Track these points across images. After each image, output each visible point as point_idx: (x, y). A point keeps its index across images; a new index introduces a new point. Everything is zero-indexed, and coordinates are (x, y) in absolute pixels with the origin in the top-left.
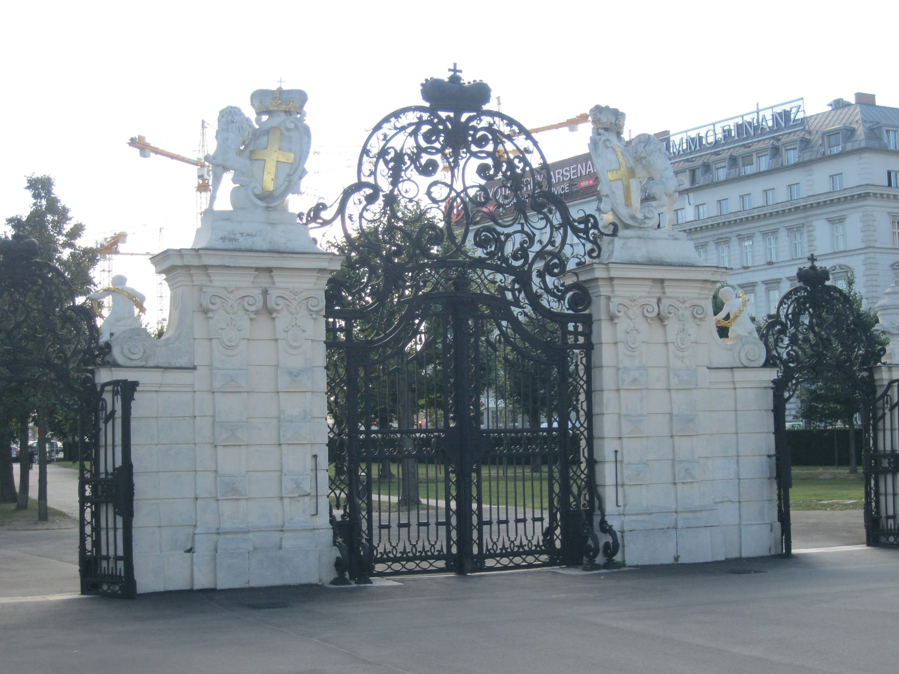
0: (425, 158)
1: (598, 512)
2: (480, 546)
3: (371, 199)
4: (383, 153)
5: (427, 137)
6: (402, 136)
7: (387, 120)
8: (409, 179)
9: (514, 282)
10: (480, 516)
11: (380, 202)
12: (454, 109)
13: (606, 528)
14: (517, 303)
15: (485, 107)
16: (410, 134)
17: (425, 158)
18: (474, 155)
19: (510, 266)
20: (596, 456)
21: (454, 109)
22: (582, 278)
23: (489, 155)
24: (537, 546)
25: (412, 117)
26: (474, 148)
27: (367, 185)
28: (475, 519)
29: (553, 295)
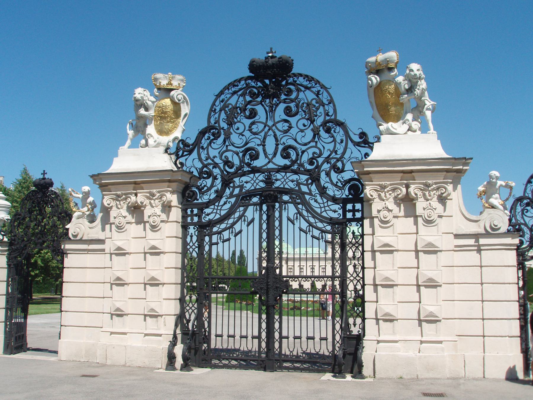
3: (216, 136)
6: (235, 97)
7: (227, 88)
8: (239, 122)
9: (307, 180)
10: (280, 333)
11: (222, 137)
14: (310, 194)
16: (240, 95)
28: (277, 335)
29: (336, 186)
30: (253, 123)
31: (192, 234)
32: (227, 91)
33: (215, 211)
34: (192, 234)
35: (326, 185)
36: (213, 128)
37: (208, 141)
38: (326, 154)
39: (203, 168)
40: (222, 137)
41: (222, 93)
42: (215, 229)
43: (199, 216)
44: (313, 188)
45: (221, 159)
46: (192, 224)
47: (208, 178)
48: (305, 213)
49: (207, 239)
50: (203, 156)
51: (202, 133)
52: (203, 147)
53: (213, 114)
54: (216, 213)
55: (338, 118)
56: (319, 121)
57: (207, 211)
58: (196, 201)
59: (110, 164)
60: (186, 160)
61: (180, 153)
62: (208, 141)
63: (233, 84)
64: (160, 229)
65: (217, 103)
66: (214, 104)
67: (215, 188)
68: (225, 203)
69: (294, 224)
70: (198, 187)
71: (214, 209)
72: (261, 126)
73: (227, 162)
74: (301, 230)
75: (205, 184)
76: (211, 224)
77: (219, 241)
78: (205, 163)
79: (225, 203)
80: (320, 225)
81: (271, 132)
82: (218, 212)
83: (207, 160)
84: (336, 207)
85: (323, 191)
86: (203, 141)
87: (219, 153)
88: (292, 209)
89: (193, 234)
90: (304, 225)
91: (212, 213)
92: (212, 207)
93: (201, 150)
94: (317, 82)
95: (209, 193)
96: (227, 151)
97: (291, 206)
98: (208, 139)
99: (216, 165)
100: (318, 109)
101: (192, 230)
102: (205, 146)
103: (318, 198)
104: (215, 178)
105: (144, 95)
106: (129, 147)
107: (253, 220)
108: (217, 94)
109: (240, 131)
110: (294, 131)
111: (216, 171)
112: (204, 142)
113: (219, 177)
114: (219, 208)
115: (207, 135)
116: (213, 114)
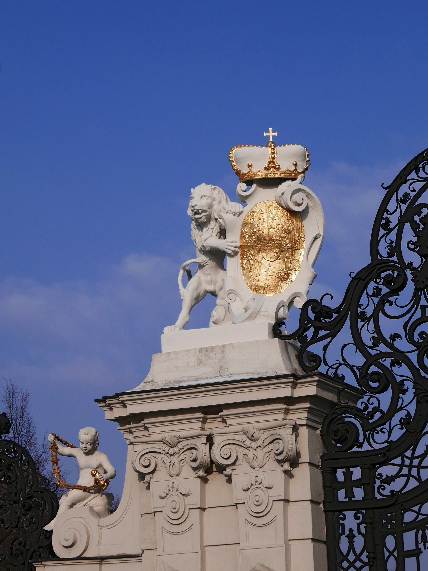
31: (351, 530)
32: (413, 175)
33: (405, 471)
34: (351, 530)
36: (385, 264)
37: (376, 300)
39: (367, 366)
41: (401, 179)
42: (409, 517)
43: (367, 482)
45: (411, 341)
46: (351, 505)
47: (383, 390)
49: (390, 542)
50: (367, 337)
51: (359, 282)
52: (363, 313)
53: (382, 232)
54: (409, 475)
58: (355, 449)
59: (144, 368)
60: (325, 348)
61: (310, 333)
62: (376, 300)
64: (273, 520)
65: (392, 205)
66: (383, 208)
67: (402, 414)
70: (358, 413)
71: (402, 466)
75: (376, 404)
77: (421, 546)
82: (414, 472)
83: (376, 345)
86: (364, 300)
87: (405, 327)
89: (355, 532)
91: (398, 475)
92: (398, 461)
93: (360, 323)
95: (387, 426)
98: (374, 295)
99: (399, 358)
101: (350, 521)
102: (369, 312)
104: (399, 389)
105: (214, 200)
106: (186, 327)
108: (388, 183)
111: (402, 371)
112: (367, 304)
114: (416, 462)
115: (372, 285)
116: (382, 232)
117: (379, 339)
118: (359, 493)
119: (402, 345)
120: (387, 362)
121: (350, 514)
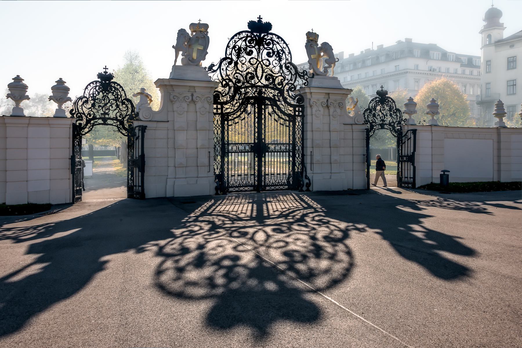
0: (249, 49)
1: (304, 172)
2: (265, 182)
3: (230, 63)
4: (234, 47)
5: (249, 42)
6: (240, 41)
7: (236, 35)
9: (278, 93)
11: (233, 65)
12: (259, 32)
13: (307, 177)
14: (279, 101)
15: (270, 32)
16: (244, 41)
17: (249, 49)
18: (266, 49)
19: (277, 87)
20: (305, 153)
21: (259, 32)
22: (302, 92)
23: (271, 49)
24: (284, 183)
25: (244, 34)
26: (266, 46)
27: (229, 58)
29: (291, 98)
30: (252, 58)
35: (287, 97)
38: (286, 81)
40: (233, 65)
41: (233, 38)
44: (281, 98)
48: (277, 111)
49: (226, 122)
55: (292, 62)
56: (283, 62)
57: (226, 106)
63: (239, 33)
68: (236, 103)
69: (271, 116)
72: (255, 61)
73: (237, 79)
74: (275, 119)
76: (228, 114)
78: (225, 78)
79: (236, 103)
80: (283, 117)
81: (260, 65)
84: (291, 109)
85: (285, 99)
88: (270, 109)
90: (276, 117)
92: (229, 104)
94: (282, 40)
96: (236, 73)
97: (270, 107)
99: (230, 80)
100: (282, 54)
103: (283, 103)
104: (230, 88)
107: (250, 113)
108: (230, 38)
109: (243, 62)
110: (271, 66)
111: (230, 83)
112: (223, 66)
113: (232, 89)
117: (227, 75)
118: (219, 111)
119: (231, 78)
120: (228, 81)
121: (217, 116)
